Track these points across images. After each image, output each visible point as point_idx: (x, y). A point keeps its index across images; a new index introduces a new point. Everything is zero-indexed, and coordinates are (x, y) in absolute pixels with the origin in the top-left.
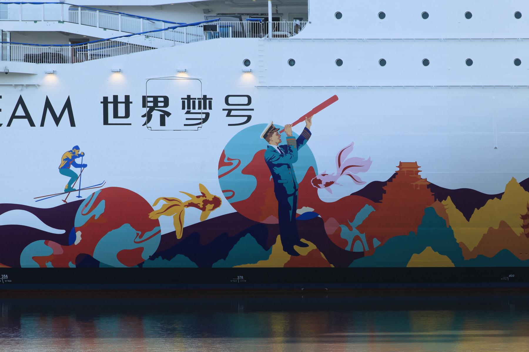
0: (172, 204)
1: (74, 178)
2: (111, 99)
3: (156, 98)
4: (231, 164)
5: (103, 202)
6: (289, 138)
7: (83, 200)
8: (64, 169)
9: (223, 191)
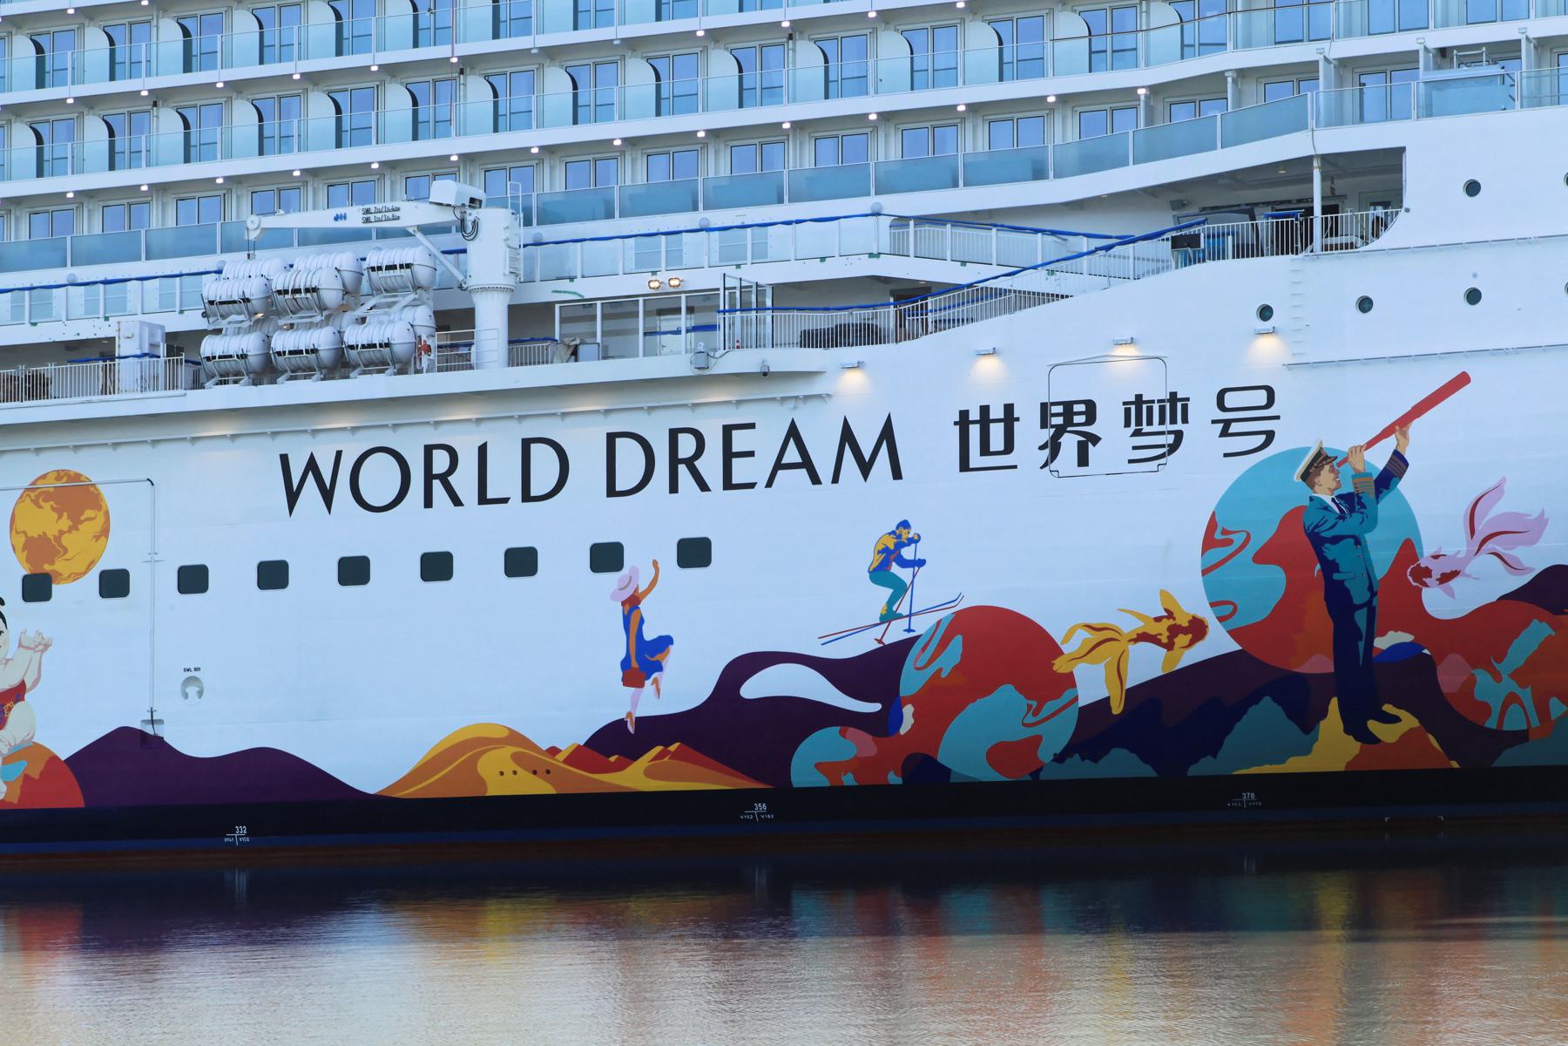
0: (1103, 637)
1: (900, 589)
2: (975, 415)
3: (1068, 406)
4: (1230, 542)
5: (958, 639)
6: (1359, 476)
7: (917, 638)
8: (880, 573)
9: (1212, 605)
